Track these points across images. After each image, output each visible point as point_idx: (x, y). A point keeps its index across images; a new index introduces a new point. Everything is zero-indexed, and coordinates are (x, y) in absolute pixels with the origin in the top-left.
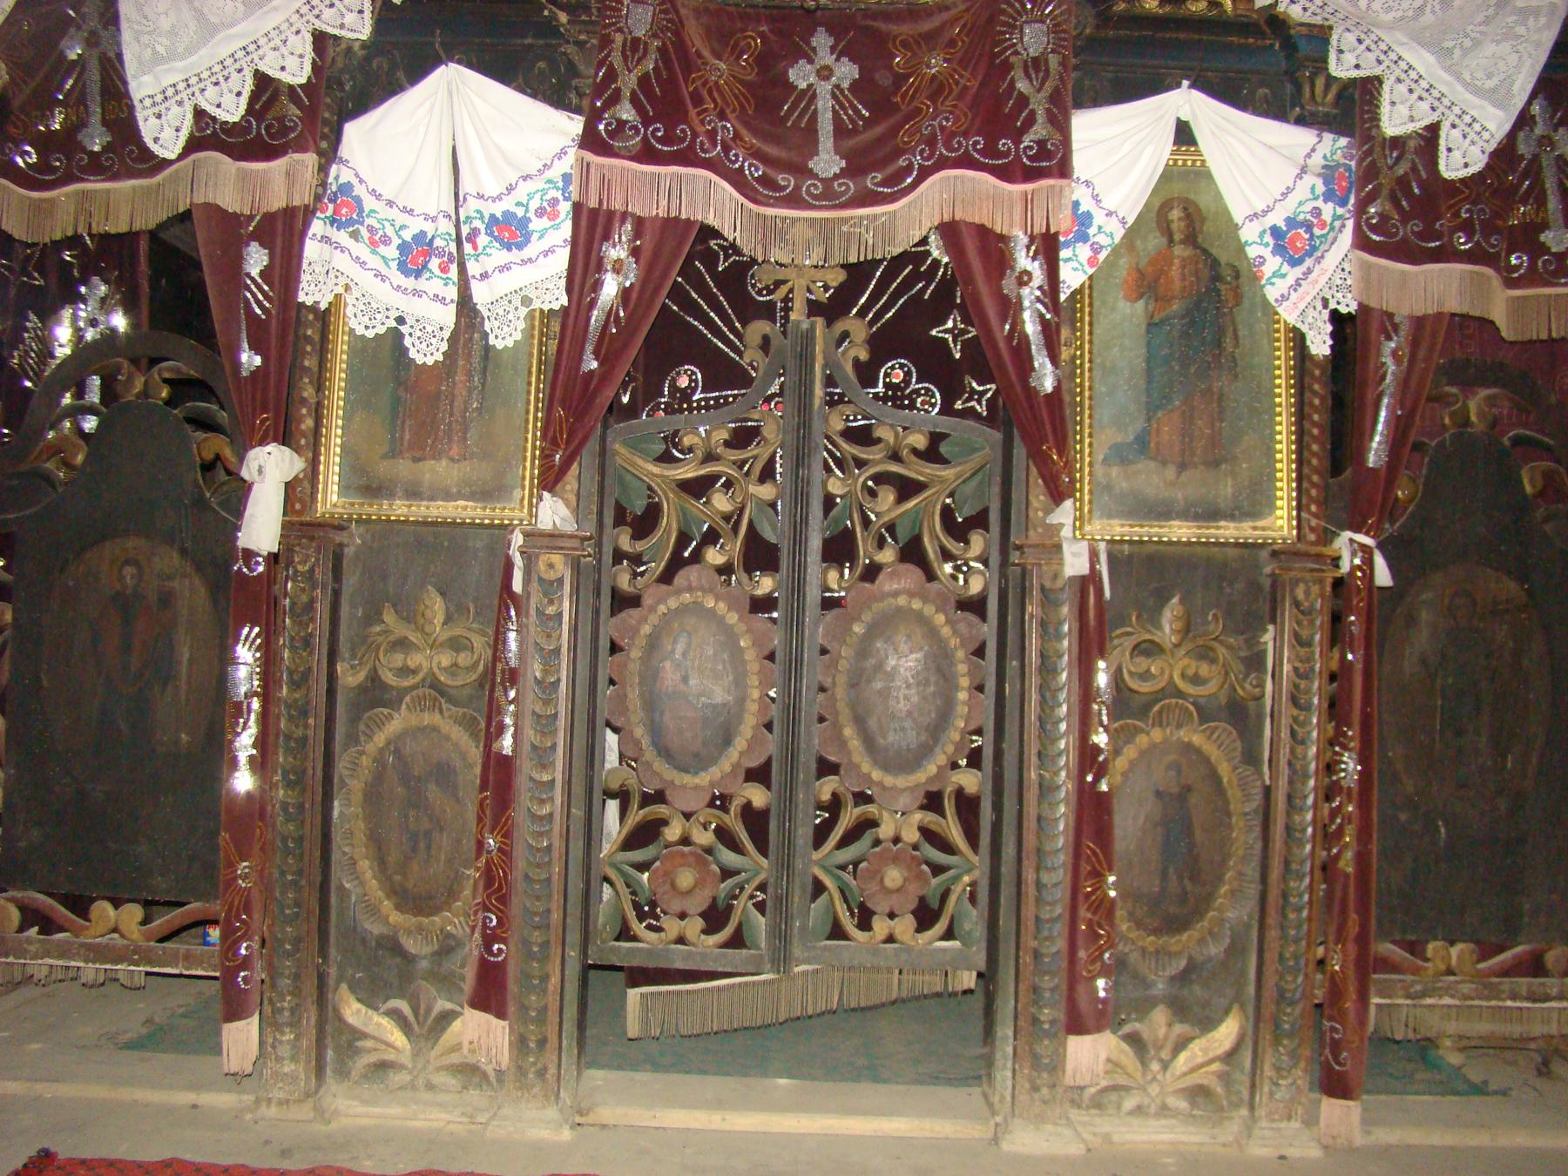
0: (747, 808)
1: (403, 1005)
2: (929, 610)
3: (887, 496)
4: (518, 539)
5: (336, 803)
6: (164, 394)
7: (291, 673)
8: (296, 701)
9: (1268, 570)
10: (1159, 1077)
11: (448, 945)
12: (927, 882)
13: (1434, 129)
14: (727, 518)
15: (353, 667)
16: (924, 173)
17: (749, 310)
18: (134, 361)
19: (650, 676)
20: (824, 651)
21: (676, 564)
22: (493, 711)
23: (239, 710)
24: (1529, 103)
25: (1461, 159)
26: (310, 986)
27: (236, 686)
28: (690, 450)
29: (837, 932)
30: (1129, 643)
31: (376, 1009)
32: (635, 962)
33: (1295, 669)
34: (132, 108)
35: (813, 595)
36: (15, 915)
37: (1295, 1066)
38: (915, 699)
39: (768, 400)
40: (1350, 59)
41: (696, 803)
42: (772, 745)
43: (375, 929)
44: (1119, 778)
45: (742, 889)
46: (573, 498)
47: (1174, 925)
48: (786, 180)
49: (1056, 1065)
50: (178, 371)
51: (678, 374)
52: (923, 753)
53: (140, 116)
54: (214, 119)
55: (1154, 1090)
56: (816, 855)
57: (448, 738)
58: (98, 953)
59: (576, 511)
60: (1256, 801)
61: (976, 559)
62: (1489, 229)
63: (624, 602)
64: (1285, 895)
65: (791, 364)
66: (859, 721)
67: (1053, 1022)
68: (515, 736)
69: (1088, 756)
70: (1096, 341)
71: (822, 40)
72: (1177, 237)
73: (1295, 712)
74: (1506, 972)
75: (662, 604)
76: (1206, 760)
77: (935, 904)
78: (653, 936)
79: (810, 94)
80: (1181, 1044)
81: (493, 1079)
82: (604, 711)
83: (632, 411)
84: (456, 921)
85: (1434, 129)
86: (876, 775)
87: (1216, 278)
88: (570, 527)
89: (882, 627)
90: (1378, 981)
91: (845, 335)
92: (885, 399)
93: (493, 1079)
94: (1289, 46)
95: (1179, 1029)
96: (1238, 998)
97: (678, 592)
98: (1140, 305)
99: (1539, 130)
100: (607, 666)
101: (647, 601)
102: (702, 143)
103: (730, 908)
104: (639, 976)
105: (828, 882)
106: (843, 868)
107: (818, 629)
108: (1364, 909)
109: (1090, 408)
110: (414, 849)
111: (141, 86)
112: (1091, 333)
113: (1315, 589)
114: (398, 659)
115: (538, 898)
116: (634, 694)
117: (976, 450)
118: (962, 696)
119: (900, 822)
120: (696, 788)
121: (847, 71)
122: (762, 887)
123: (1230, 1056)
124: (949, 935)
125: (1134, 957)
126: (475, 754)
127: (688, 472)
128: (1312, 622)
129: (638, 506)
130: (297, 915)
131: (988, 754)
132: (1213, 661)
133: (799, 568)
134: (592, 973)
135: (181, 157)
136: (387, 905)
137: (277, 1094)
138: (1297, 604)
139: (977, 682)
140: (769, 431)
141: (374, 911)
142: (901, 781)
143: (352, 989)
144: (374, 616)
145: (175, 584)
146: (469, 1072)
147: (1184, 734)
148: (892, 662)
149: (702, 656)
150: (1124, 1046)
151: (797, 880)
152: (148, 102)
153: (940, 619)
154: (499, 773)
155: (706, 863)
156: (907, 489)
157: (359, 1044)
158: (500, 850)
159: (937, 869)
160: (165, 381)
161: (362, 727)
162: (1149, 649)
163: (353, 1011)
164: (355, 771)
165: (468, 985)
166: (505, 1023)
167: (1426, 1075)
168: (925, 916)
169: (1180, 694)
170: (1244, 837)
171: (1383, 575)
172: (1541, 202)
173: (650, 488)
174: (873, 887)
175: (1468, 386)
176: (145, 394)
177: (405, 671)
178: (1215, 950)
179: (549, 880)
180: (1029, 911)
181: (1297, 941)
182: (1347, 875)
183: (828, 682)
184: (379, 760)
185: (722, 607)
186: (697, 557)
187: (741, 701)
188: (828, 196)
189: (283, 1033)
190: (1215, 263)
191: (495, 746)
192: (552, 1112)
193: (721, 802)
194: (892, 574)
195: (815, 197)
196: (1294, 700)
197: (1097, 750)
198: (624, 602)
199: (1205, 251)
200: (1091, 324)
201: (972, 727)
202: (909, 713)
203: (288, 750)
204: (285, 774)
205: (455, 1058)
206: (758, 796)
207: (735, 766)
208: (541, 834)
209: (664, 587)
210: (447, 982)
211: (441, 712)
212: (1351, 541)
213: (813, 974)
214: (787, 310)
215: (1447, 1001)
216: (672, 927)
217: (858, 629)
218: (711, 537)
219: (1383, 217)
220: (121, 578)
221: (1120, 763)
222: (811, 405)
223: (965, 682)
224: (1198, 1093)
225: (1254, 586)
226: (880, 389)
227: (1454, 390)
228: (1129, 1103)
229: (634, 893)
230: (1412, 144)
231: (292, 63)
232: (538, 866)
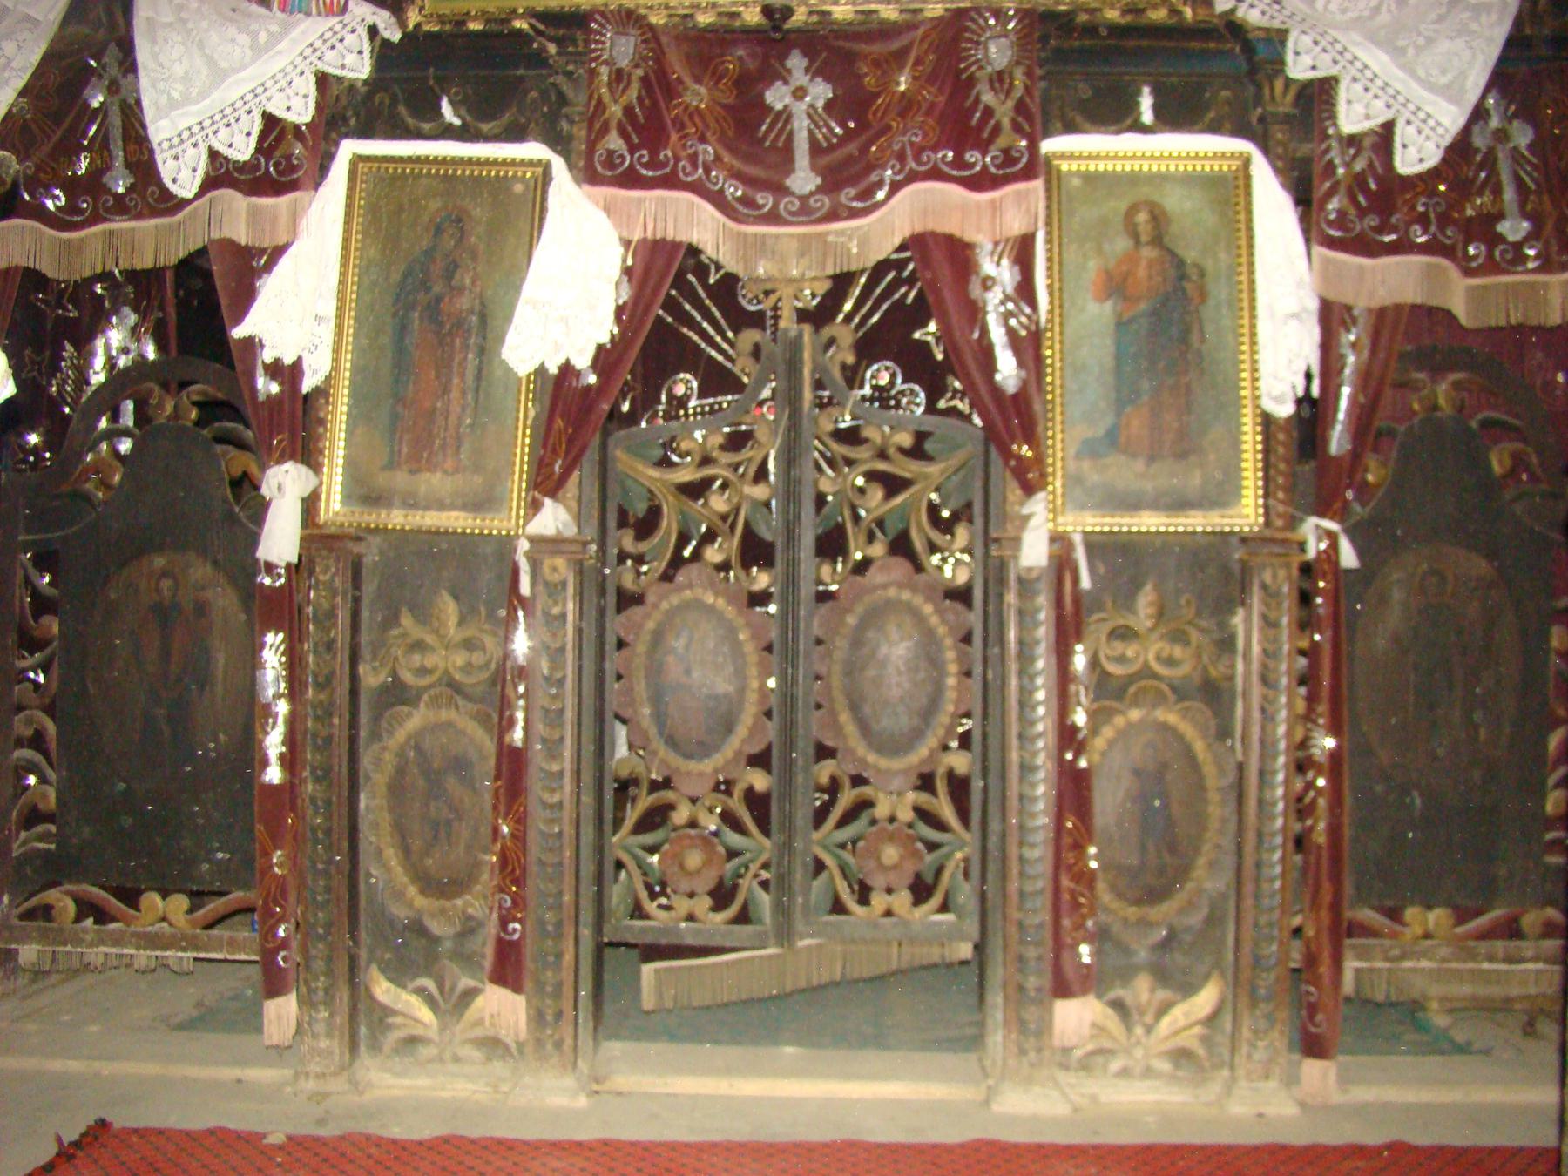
0: (750, 794)
1: (429, 983)
2: (918, 600)
3: (877, 494)
4: (524, 545)
5: (362, 796)
6: (194, 415)
7: (315, 676)
8: (321, 702)
9: (1237, 556)
10: (1143, 1040)
11: (469, 928)
12: (921, 858)
13: (1389, 127)
14: (724, 518)
15: (374, 669)
16: (895, 187)
17: (742, 320)
18: (165, 386)
19: (655, 670)
20: (819, 642)
21: (677, 562)
22: (505, 705)
24: (1483, 97)
25: (1416, 154)
26: (342, 966)
27: (264, 689)
28: (688, 454)
29: (838, 907)
30: (1106, 628)
31: (404, 987)
32: (649, 939)
33: (1265, 651)
34: (151, 152)
35: (806, 590)
36: (71, 907)
37: (1272, 1027)
38: (907, 685)
39: (761, 404)
40: (1307, 60)
41: (701, 788)
42: (772, 730)
43: (400, 912)
44: (1096, 758)
45: (747, 868)
46: (574, 505)
47: (1154, 895)
48: (765, 200)
49: (1044, 1028)
50: (205, 393)
51: (675, 382)
52: (916, 735)
53: (159, 158)
54: (226, 158)
55: (1139, 1053)
56: (816, 835)
57: (463, 732)
58: (153, 941)
59: (579, 518)
60: (1231, 776)
61: (962, 551)
62: (1444, 220)
63: (628, 600)
64: (1258, 865)
65: (781, 368)
66: (855, 708)
67: (1039, 990)
68: (526, 729)
69: (1068, 736)
70: (1067, 342)
71: (796, 62)
72: (1144, 238)
73: (1265, 691)
74: (1483, 936)
75: (664, 601)
76: (1180, 738)
77: (929, 879)
78: (663, 914)
79: (785, 116)
80: (1163, 1009)
81: (515, 1053)
82: (613, 703)
83: (632, 419)
84: (477, 903)
85: (1389, 127)
86: (872, 758)
87: (1183, 277)
88: (571, 531)
89: (875, 617)
90: (1353, 947)
91: (832, 341)
92: (872, 400)
93: (515, 1053)
94: (1249, 49)
95: (1162, 994)
96: (1218, 965)
97: (680, 589)
98: (1108, 306)
99: (1495, 122)
100: (613, 661)
101: (651, 598)
102: (684, 168)
103: (735, 887)
104: (653, 952)
105: (829, 860)
106: (843, 846)
107: (813, 622)
108: (1336, 879)
109: (1062, 405)
110: (436, 836)
111: (159, 130)
112: (1061, 333)
113: (1282, 573)
114: (417, 659)
115: (551, 880)
116: (641, 689)
117: (959, 447)
118: (951, 681)
119: (895, 802)
120: (701, 774)
121: (821, 92)
122: (766, 866)
123: (1212, 1020)
124: (944, 908)
125: (1116, 928)
126: (490, 746)
127: (686, 475)
128: (1279, 604)
129: (640, 508)
130: (328, 901)
131: (976, 738)
132: (1187, 643)
133: (793, 564)
134: (608, 951)
135: (199, 195)
136: (412, 890)
137: (314, 1068)
138: (1264, 587)
139: (965, 669)
140: (762, 434)
141: (399, 895)
143: (383, 971)
144: (392, 620)
145: (209, 594)
146: (493, 1045)
147: (1161, 715)
148: (884, 650)
149: (706, 649)
150: (1110, 1011)
151: (798, 861)
152: (166, 145)
153: (928, 609)
154: (512, 764)
155: (713, 846)
156: (893, 485)
157: (390, 1020)
158: (513, 835)
159: (932, 846)
160: (195, 404)
161: (384, 724)
162: (1123, 634)
163: (383, 989)
165: (488, 963)
166: (520, 1001)
167: (1409, 1037)
169: (1155, 676)
170: (1217, 809)
171: (1348, 557)
172: (1497, 191)
173: (650, 491)
174: (872, 864)
175: (1437, 372)
176: (176, 415)
177: (423, 671)
178: (1195, 919)
179: (560, 864)
180: (1013, 886)
181: (1271, 909)
182: (1319, 847)
183: (823, 670)
184: (401, 754)
185: (721, 602)
186: (697, 555)
187: (742, 690)
188: (805, 212)
189: (318, 1011)
190: (1180, 263)
191: (507, 739)
192: (569, 1081)
193: (725, 787)
194: (882, 568)
195: (792, 214)
196: (1264, 681)
197: (1074, 729)
198: (628, 600)
199: (1173, 254)
200: (1061, 324)
201: (963, 709)
202: (902, 699)
203: (317, 748)
204: (313, 772)
205: (479, 1032)
206: (760, 781)
207: (738, 753)
208: (552, 821)
209: (666, 585)
210: (468, 961)
211: (457, 707)
212: (1317, 527)
213: (816, 949)
214: (776, 318)
215: (1424, 964)
216: (683, 905)
217: (851, 620)
218: (709, 537)
219: (1341, 213)
220: (158, 591)
221: (1099, 743)
222: (801, 408)
223: (953, 668)
224: (1181, 1056)
225: (1225, 571)
226: (867, 391)
227: (1421, 376)
228: (1116, 1065)
229: (645, 874)
230: (1367, 143)
231: (297, 103)
232: (551, 850)
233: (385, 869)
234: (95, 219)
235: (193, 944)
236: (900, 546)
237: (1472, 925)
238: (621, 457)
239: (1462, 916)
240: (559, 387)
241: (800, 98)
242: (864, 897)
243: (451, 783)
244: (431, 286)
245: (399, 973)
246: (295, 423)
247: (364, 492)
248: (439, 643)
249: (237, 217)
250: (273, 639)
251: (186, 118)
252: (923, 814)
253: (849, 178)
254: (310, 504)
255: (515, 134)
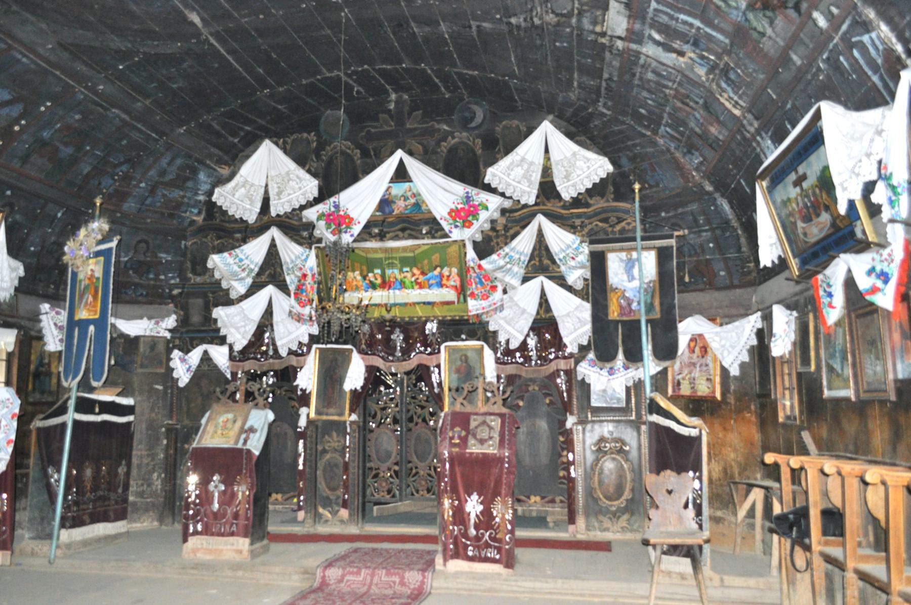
11: (338, 498)
21: (380, 423)
23: (300, 455)
25: (514, 345)
29: (413, 494)
42: (398, 457)
43: (324, 494)
48: (391, 358)
59: (359, 417)
66: (416, 454)
71: (398, 330)
100: (368, 443)
104: (376, 504)
111: (279, 343)
129: (373, 413)
142: (423, 464)
144: (323, 437)
146: (342, 521)
154: (346, 465)
163: (321, 510)
164: (321, 464)
168: (429, 491)
188: (399, 360)
206: (396, 468)
210: (337, 504)
233: (322, 485)
234: (266, 360)
235: (282, 504)
236: (424, 420)
237: (546, 499)
238: (369, 403)
239: (543, 498)
240: (354, 392)
241: (398, 338)
242: (417, 491)
243: (335, 469)
244: (331, 373)
245: (324, 507)
246: (304, 399)
247: (318, 412)
248: (332, 441)
249: (294, 361)
250: (301, 442)
251: (284, 341)
252: (430, 475)
253: (406, 352)
254: (308, 415)
255: (345, 343)
